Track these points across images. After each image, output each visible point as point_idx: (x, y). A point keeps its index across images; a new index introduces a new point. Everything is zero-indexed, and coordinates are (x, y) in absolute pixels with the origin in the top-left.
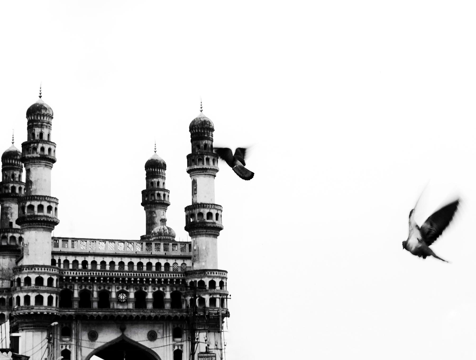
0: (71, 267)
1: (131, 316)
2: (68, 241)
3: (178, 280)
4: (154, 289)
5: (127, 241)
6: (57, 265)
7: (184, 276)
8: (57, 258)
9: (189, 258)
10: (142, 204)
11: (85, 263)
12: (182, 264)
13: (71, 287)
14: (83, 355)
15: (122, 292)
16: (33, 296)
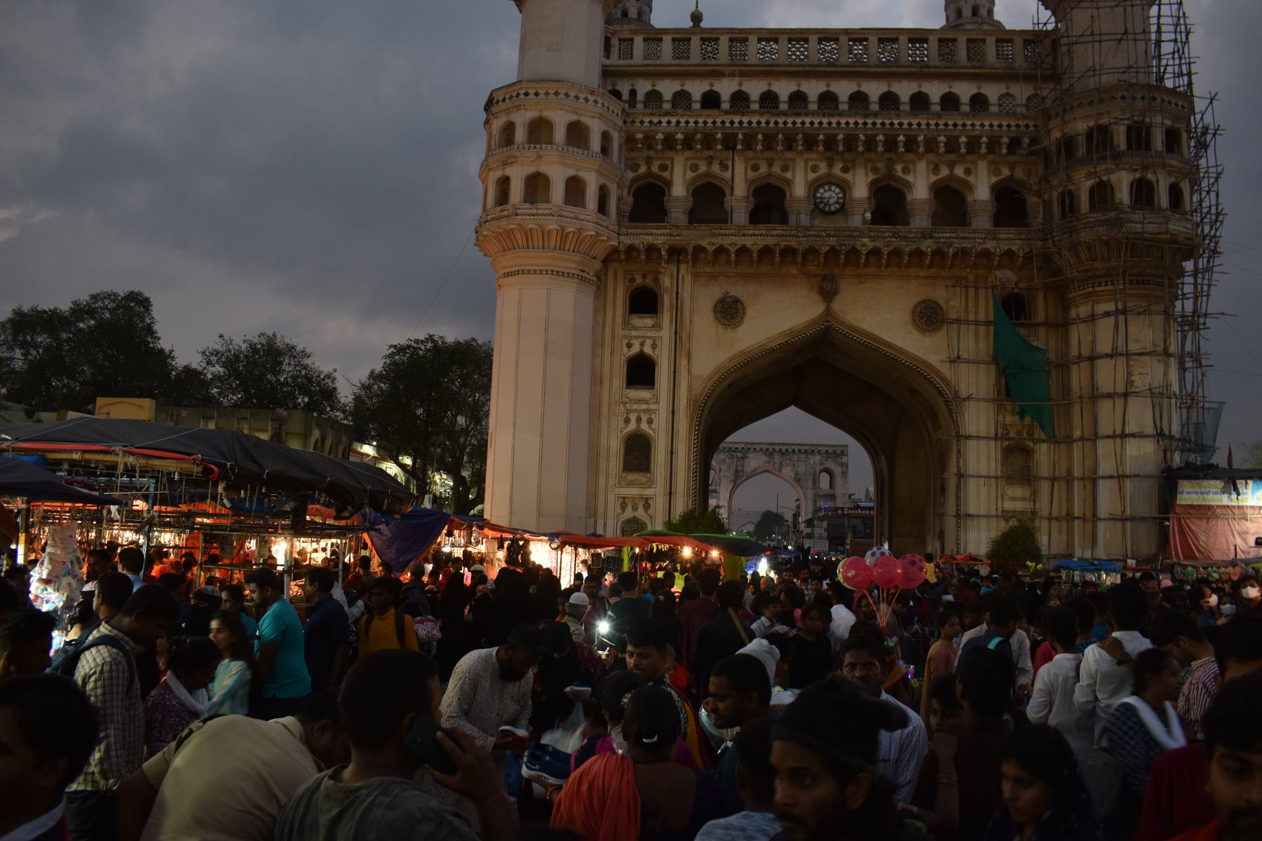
0: (667, 106)
1: (854, 252)
2: (661, 40)
3: (1014, 143)
4: (936, 169)
5: (846, 32)
6: (627, 106)
7: (1035, 126)
8: (624, 87)
9: (1054, 77)
11: (711, 100)
12: (1029, 98)
13: (663, 168)
14: (695, 372)
15: (828, 181)
16: (518, 176)
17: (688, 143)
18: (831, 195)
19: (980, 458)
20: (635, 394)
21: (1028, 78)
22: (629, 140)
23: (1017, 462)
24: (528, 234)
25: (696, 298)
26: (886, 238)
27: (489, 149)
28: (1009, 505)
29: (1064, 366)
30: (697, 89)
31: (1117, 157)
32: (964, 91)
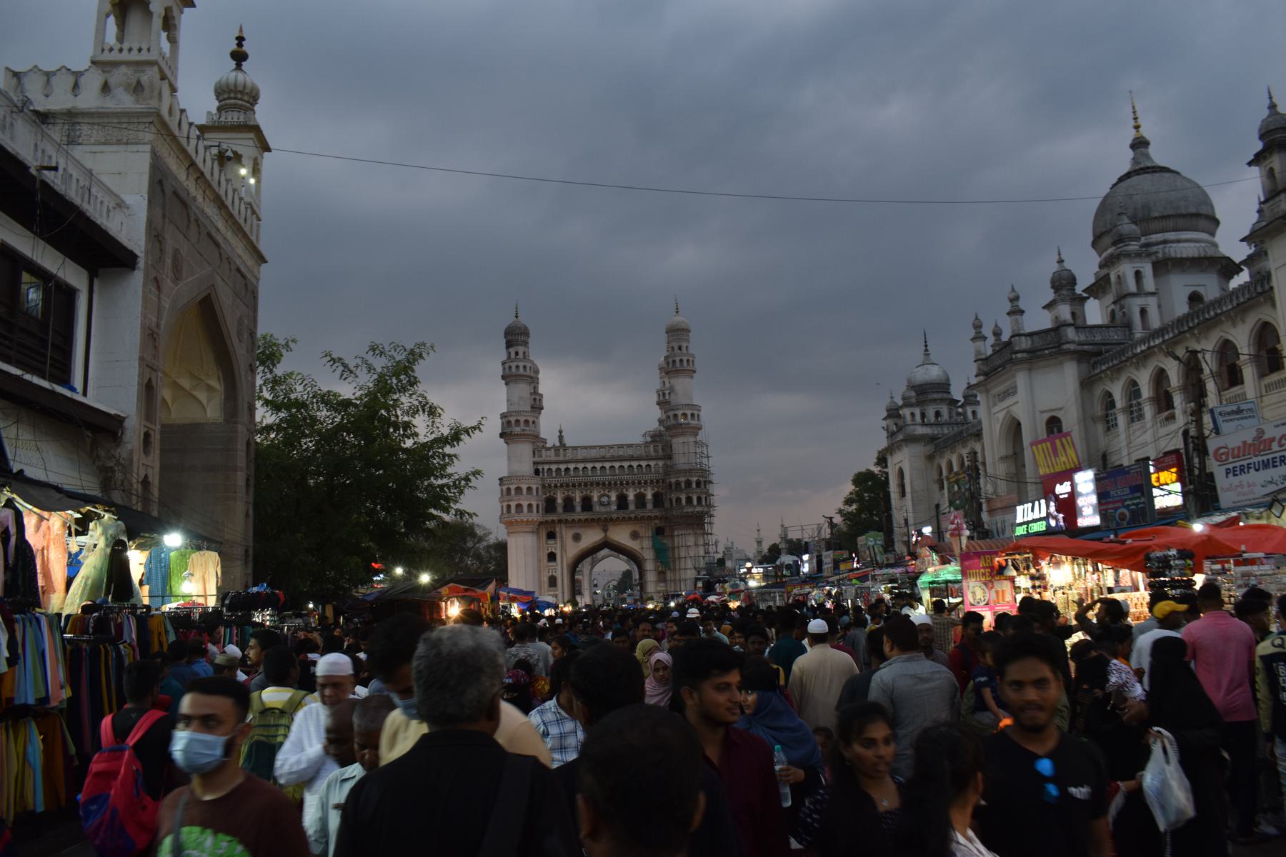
1: (611, 519)
3: (658, 482)
10: (658, 404)
15: (604, 495)
16: (513, 504)
19: (651, 577)
23: (662, 576)
26: (622, 514)
29: (673, 548)
30: (563, 467)
31: (681, 490)
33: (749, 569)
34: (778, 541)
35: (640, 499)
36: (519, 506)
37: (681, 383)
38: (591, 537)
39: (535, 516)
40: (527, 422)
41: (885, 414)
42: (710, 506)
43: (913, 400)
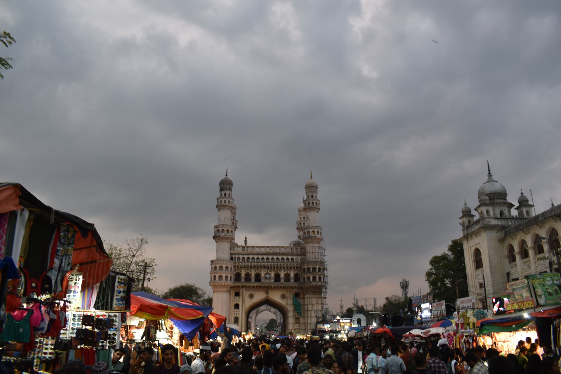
1: (271, 287)
3: (297, 267)
15: (268, 273)
16: (217, 275)
17: (245, 267)
18: (268, 276)
19: (291, 320)
20: (236, 310)
21: (300, 255)
22: (235, 267)
24: (219, 285)
25: (245, 294)
26: (277, 284)
27: (212, 270)
28: (295, 327)
29: (304, 305)
30: (246, 257)
32: (290, 257)
33: (338, 320)
34: (351, 306)
35: (287, 276)
36: (220, 277)
37: (312, 215)
38: (259, 296)
39: (229, 283)
40: (228, 231)
41: (461, 214)
42: (326, 283)
43: (488, 202)
